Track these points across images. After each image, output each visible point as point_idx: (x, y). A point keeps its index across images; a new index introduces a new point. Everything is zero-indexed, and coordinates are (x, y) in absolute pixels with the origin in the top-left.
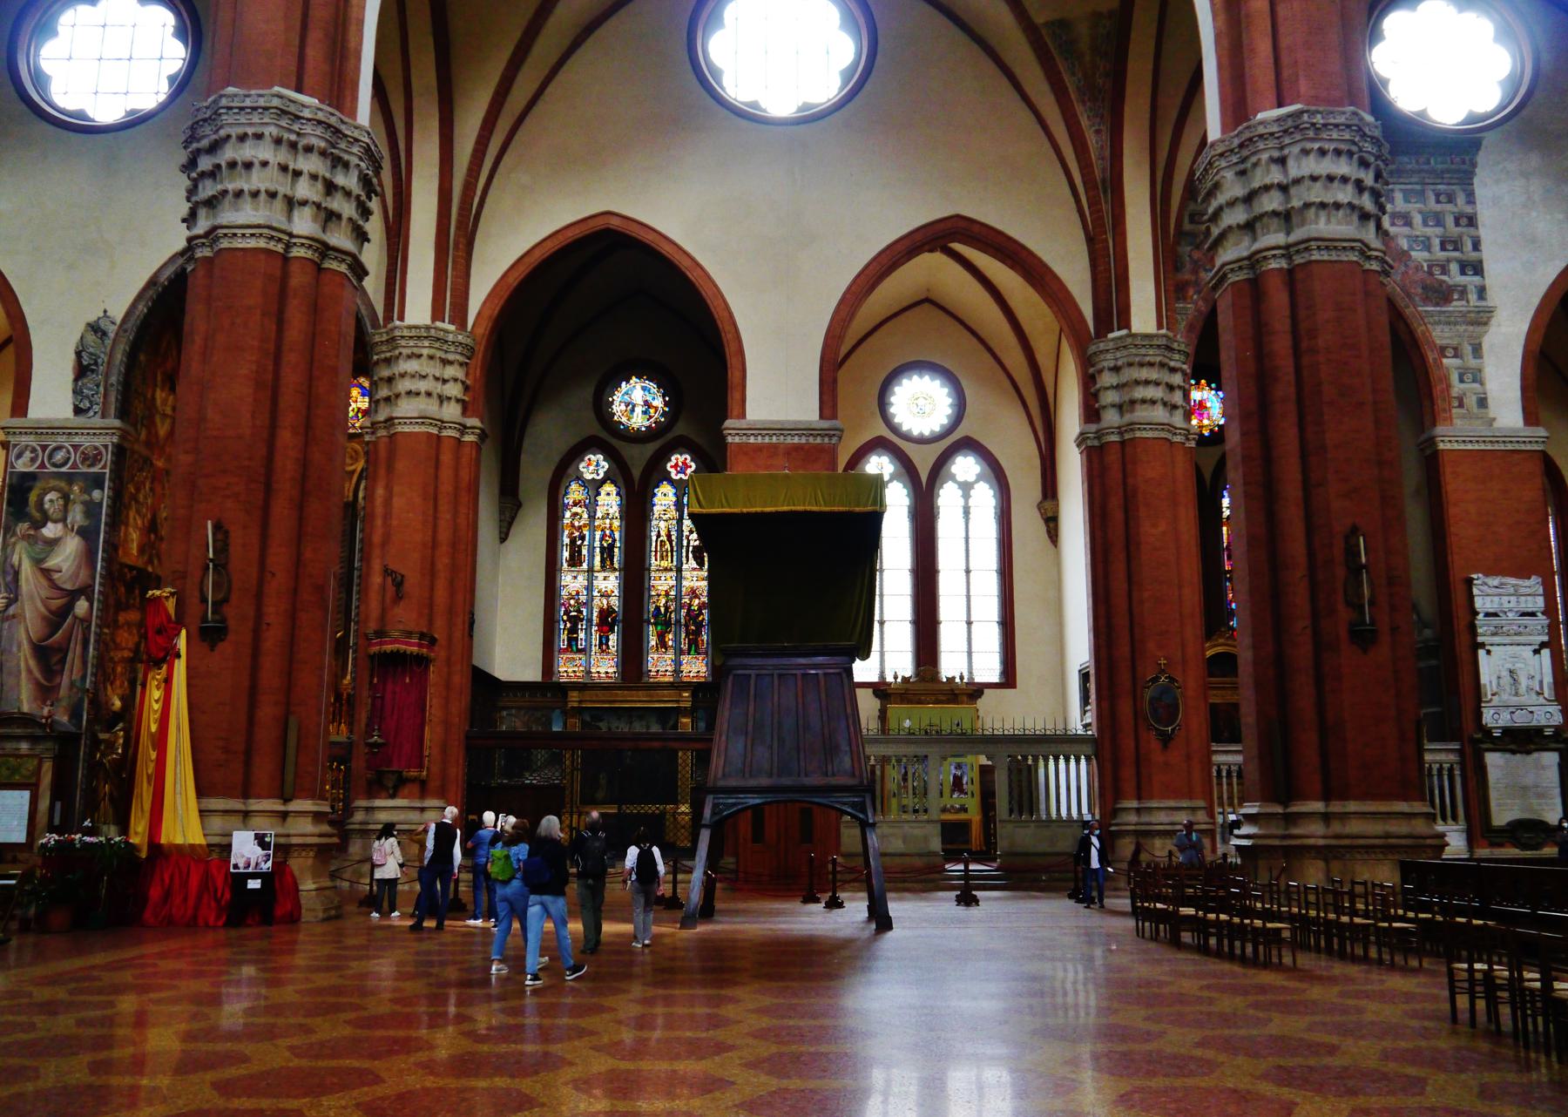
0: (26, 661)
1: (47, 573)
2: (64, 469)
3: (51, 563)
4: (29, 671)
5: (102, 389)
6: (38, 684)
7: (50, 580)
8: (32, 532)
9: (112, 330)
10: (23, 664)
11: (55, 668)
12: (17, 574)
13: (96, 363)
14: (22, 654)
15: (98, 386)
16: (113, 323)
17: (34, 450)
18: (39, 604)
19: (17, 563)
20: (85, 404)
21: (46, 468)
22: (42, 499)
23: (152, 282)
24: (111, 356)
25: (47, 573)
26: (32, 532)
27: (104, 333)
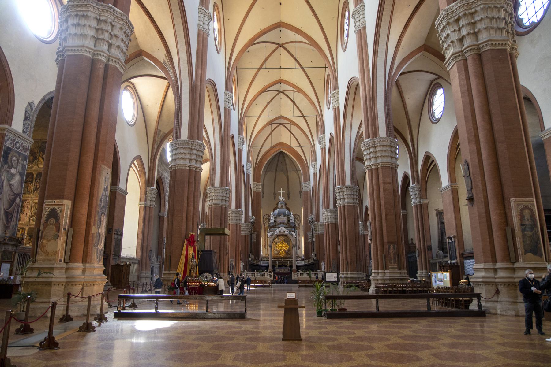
0: (2, 215)
1: (10, 185)
2: (18, 150)
3: (12, 182)
4: (3, 220)
5: (30, 127)
6: (4, 225)
7: (11, 188)
8: (8, 169)
9: (34, 108)
10: (1, 217)
11: (9, 220)
12: (3, 183)
13: (29, 117)
14: (1, 213)
15: (29, 125)
16: (35, 106)
17: (11, 140)
18: (8, 196)
19: (3, 180)
20: (25, 130)
21: (14, 148)
22: (12, 159)
23: (44, 98)
24: (33, 116)
25: (10, 185)
26: (8, 169)
27: (32, 109)
